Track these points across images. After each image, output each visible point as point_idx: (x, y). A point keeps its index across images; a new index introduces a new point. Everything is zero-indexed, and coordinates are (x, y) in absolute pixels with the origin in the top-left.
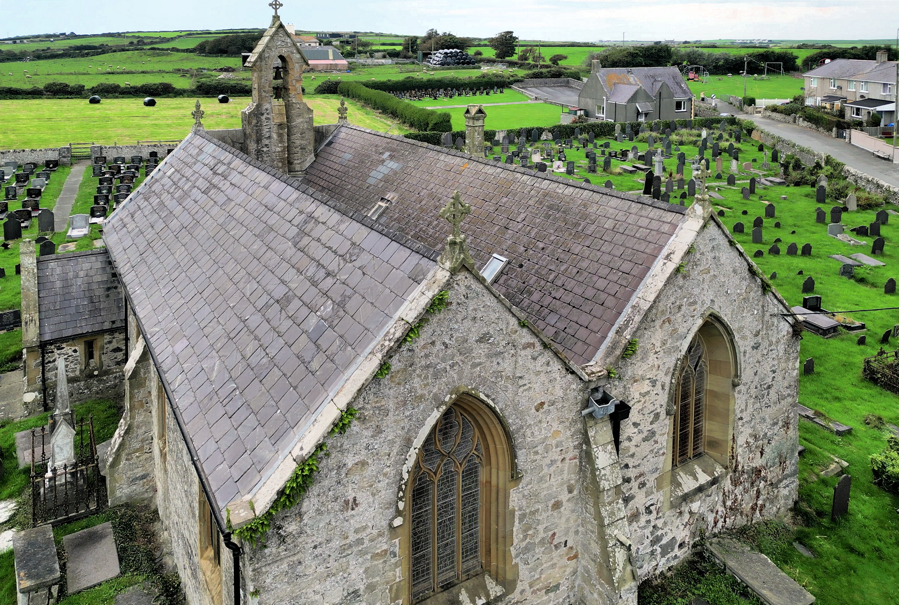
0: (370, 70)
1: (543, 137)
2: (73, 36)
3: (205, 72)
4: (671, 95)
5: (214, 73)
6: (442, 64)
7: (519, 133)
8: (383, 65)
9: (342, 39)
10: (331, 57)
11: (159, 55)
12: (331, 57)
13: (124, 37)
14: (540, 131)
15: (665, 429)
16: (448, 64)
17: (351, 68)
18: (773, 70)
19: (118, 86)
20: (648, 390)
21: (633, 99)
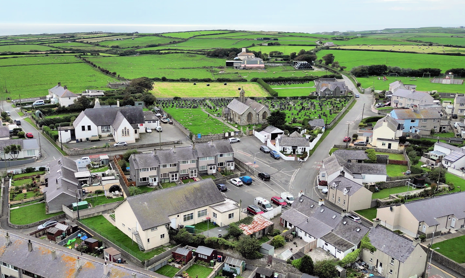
0: (272, 69)
3: (214, 69)
4: (339, 89)
5: (216, 69)
6: (299, 68)
7: (292, 97)
8: (278, 66)
9: (270, 42)
10: (258, 63)
11: (192, 56)
12: (258, 63)
13: (165, 37)
14: (298, 97)
15: (262, 117)
16: (301, 68)
17: (265, 68)
18: (426, 76)
20: (261, 114)
21: (325, 90)
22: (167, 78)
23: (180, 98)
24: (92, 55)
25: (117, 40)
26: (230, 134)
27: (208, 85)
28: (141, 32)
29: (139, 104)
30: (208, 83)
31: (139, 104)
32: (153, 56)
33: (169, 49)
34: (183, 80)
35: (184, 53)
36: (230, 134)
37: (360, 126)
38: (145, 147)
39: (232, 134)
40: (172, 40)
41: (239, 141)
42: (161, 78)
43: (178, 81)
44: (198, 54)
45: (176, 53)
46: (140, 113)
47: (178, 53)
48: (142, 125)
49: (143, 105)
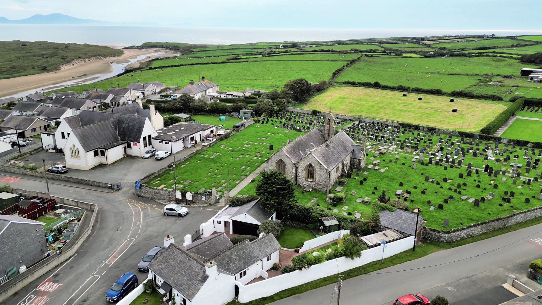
1: (529, 145)
2: (493, 37)
7: (514, 141)
11: (499, 61)
19: (421, 89)
22: (382, 83)
23: (319, 112)
24: (396, 55)
25: (458, 42)
26: (184, 195)
27: (420, 99)
28: (497, 35)
29: (244, 113)
30: (420, 96)
31: (244, 113)
32: (463, 58)
33: (493, 52)
34: (401, 89)
35: (496, 56)
36: (184, 195)
37: (533, 266)
38: (72, 182)
39: (189, 196)
40: (515, 43)
41: (180, 215)
42: (373, 83)
43: (393, 89)
44: (512, 58)
45: (487, 56)
46: (140, 127)
47: (489, 56)
48: (137, 145)
49: (250, 115)
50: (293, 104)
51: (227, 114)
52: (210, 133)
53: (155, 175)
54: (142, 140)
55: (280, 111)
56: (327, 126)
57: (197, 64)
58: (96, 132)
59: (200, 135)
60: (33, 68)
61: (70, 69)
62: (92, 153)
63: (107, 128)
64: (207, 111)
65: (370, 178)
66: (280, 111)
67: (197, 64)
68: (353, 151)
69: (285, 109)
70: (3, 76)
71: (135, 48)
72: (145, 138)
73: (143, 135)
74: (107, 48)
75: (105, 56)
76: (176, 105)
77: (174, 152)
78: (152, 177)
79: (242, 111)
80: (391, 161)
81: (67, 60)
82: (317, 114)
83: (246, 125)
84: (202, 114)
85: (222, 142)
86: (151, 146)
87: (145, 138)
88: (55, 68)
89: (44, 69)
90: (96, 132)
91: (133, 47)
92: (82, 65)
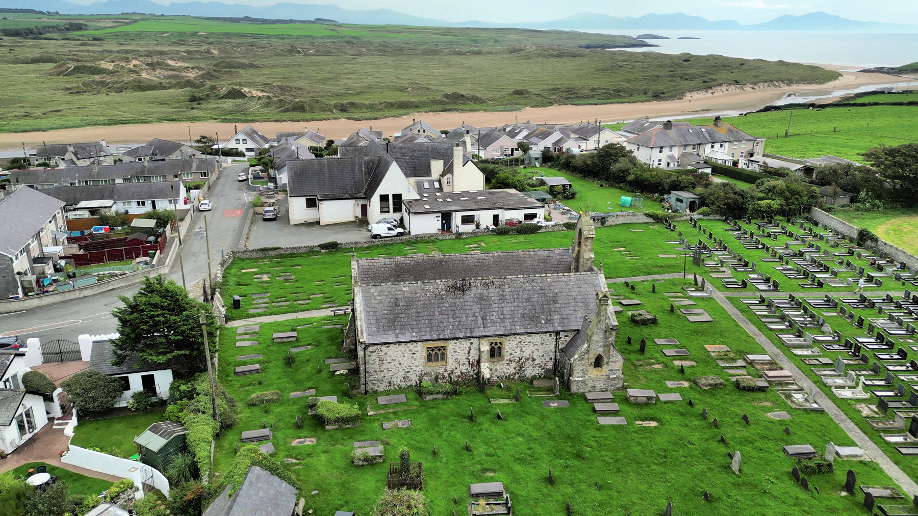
50: (868, 205)
51: (656, 195)
52: (522, 218)
53: (282, 252)
54: (375, 200)
55: (782, 212)
56: (577, 249)
57: (910, 104)
58: (326, 171)
59: (496, 218)
60: (646, 93)
61: (701, 99)
62: (303, 200)
63: (353, 170)
64: (630, 183)
65: (532, 420)
66: (782, 212)
67: (910, 104)
68: (578, 331)
69: (808, 209)
70: (591, 101)
71: (884, 73)
72: (384, 198)
73: (382, 190)
74: (813, 68)
75: (790, 82)
76: (589, 162)
77: (412, 234)
78: (272, 253)
79: (675, 194)
80: (704, 415)
81: (707, 85)
82: (869, 243)
83: (610, 221)
84: (620, 188)
85: (496, 239)
86: (397, 216)
87: (384, 198)
88: (676, 95)
89: (657, 96)
90: (326, 171)
91: (880, 70)
92: (737, 94)
